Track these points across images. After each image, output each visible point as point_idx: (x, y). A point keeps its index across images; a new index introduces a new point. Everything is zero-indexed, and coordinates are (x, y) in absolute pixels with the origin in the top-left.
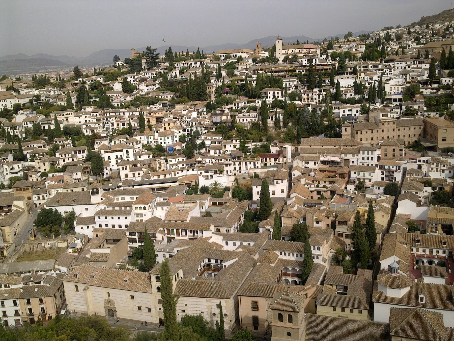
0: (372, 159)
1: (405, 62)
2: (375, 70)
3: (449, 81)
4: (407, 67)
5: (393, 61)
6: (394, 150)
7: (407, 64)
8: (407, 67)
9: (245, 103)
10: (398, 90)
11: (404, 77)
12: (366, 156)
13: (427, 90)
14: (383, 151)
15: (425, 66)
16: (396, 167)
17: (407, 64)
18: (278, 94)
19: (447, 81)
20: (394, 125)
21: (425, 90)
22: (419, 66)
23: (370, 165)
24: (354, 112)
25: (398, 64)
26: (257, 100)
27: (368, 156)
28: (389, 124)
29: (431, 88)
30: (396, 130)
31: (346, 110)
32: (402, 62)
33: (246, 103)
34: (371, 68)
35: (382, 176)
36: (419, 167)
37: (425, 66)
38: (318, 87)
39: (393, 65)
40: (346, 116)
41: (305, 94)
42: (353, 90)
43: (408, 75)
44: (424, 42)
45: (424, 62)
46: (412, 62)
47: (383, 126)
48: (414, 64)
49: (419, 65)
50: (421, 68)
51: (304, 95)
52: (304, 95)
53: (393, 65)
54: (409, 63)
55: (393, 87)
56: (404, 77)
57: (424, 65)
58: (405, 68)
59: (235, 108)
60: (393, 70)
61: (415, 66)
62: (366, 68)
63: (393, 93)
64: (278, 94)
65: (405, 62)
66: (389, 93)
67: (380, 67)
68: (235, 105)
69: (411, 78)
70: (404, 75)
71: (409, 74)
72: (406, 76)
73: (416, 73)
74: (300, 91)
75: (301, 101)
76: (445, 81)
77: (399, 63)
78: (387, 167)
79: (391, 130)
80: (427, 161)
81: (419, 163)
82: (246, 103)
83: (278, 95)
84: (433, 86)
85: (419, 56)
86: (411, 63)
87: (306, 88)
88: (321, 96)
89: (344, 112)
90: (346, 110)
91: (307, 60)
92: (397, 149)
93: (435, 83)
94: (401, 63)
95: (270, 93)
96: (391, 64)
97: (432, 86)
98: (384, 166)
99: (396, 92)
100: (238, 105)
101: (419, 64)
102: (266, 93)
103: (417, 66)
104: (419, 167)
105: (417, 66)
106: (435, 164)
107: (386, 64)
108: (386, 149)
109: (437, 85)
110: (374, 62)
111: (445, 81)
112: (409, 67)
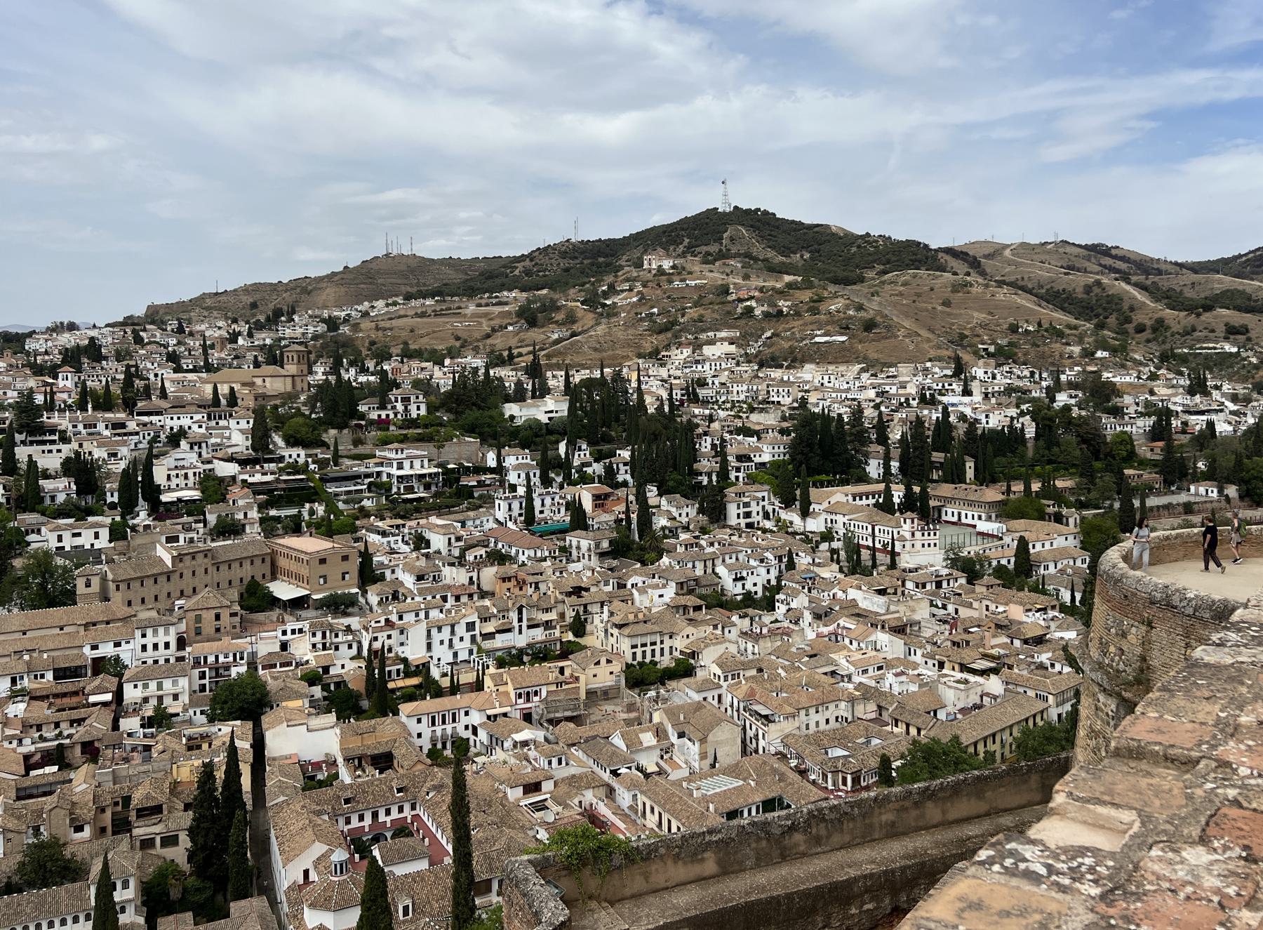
0: (167, 645)
2: (119, 435)
3: (298, 456)
4: (195, 427)
5: (158, 413)
6: (218, 617)
7: (195, 419)
8: (195, 427)
11: (196, 448)
12: (150, 640)
14: (192, 623)
15: (238, 423)
16: (235, 655)
17: (195, 419)
19: (294, 456)
20: (206, 560)
22: (223, 423)
23: (162, 662)
24: (86, 540)
25: (172, 419)
27: (155, 640)
28: (194, 558)
30: (212, 570)
31: (67, 535)
32: (181, 416)
34: (107, 427)
35: (203, 682)
36: (284, 646)
37: (238, 423)
40: (68, 548)
42: (72, 484)
43: (204, 445)
45: (231, 416)
47: (181, 565)
48: (209, 418)
50: (228, 428)
54: (197, 417)
55: (173, 473)
56: (196, 448)
57: (235, 421)
58: (190, 428)
61: (213, 423)
65: (189, 416)
67: (132, 426)
69: (210, 451)
73: (218, 440)
76: (290, 456)
77: (175, 417)
78: (211, 659)
79: (200, 571)
80: (301, 631)
81: (284, 638)
89: (60, 539)
90: (67, 535)
92: (225, 614)
94: (179, 418)
96: (154, 419)
97: (262, 467)
98: (205, 658)
101: (220, 418)
104: (284, 646)
105: (217, 423)
106: (319, 635)
107: (145, 419)
108: (198, 619)
109: (273, 466)
110: (109, 415)
111: (290, 456)
112: (200, 427)
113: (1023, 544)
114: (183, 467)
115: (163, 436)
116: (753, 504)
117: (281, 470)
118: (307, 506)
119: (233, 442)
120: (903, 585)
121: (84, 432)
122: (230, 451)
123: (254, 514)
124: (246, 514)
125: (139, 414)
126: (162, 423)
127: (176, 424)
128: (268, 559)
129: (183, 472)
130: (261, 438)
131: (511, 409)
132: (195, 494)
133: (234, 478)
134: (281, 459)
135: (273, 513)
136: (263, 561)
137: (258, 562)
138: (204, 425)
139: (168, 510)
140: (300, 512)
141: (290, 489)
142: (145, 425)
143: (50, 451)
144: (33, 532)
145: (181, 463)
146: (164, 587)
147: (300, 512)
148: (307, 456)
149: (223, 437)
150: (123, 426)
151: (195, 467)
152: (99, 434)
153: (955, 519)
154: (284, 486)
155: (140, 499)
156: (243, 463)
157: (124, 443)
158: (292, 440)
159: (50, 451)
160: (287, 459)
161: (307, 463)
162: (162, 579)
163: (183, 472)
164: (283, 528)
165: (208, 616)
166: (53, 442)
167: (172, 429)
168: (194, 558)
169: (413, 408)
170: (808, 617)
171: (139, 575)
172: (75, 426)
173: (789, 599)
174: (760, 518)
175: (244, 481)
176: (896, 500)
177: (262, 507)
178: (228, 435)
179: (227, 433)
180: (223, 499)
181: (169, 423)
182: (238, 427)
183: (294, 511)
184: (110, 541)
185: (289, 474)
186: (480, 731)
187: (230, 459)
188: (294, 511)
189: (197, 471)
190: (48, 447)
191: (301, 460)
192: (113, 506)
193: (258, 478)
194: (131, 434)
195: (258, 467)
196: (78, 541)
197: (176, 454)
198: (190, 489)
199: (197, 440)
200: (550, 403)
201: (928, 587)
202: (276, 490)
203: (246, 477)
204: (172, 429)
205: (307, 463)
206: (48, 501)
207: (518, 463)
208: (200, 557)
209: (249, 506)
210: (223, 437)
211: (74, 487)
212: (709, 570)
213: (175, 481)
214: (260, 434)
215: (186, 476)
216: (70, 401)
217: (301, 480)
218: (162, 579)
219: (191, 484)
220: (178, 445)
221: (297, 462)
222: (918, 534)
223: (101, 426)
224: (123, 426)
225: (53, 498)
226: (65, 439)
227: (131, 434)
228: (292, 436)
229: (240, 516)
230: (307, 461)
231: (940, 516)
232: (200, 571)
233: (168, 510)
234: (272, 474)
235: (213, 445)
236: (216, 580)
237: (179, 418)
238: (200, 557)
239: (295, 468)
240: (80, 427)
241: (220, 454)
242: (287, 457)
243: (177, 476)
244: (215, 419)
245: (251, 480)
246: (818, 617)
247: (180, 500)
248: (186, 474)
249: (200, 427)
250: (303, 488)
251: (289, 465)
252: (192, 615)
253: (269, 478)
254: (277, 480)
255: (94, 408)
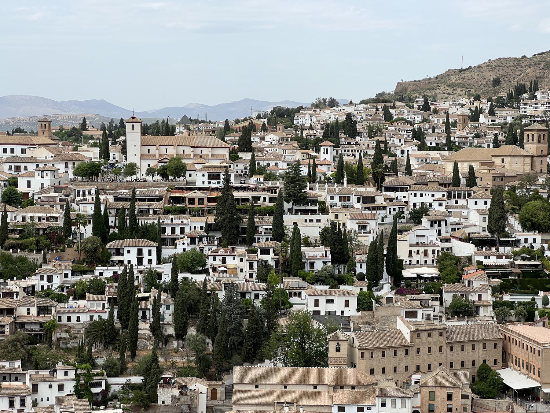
1: (431, 193)
2: (369, 208)
3: (534, 240)
4: (435, 205)
5: (403, 189)
6: (450, 397)
7: (436, 197)
8: (435, 205)
9: (66, 276)
11: (436, 225)
13: (489, 258)
14: (426, 399)
15: (476, 203)
17: (436, 197)
18: (150, 254)
19: (530, 241)
20: (441, 339)
21: (485, 258)
22: (461, 202)
24: (337, 307)
25: (415, 195)
26: (98, 269)
28: (430, 335)
29: (498, 254)
31: (322, 301)
32: (424, 193)
33: (70, 275)
34: (359, 202)
37: (476, 203)
38: (243, 242)
39: (404, 197)
41: (217, 258)
42: (328, 253)
43: (443, 223)
44: (434, 144)
45: (469, 195)
46: (446, 193)
47: (418, 340)
48: (449, 197)
49: (459, 201)
50: (466, 208)
51: (215, 259)
52: (215, 259)
53: (404, 197)
54: (438, 195)
55: (414, 249)
56: (436, 225)
58: (431, 205)
59: (42, 287)
60: (405, 208)
61: (452, 202)
62: (347, 203)
63: (414, 262)
64: (150, 254)
65: (431, 193)
66: (406, 261)
67: (380, 201)
68: (42, 278)
69: (448, 229)
70: (436, 223)
71: (446, 221)
72: (439, 226)
73: (457, 220)
74: (202, 249)
75: (206, 272)
76: (526, 240)
77: (418, 194)
79: (435, 349)
82: (70, 275)
83: (150, 257)
84: (501, 248)
85: (456, 181)
86: (444, 195)
87: (216, 243)
89: (317, 303)
90: (322, 301)
91: (206, 175)
93: (506, 243)
94: (421, 195)
95: (129, 252)
96: (400, 194)
97: (498, 250)
100: (50, 279)
101: (459, 197)
102: (119, 252)
103: (456, 202)
105: (456, 202)
107: (392, 194)
108: (432, 396)
109: (508, 249)
110: (361, 189)
111: (526, 240)
112: (440, 205)
114: (423, 244)
115: (406, 212)
117: (516, 254)
118: (541, 294)
119: (471, 222)
121: (339, 204)
122: (468, 231)
123: (488, 297)
124: (480, 296)
125: (388, 189)
126: (406, 200)
127: (418, 200)
128: (500, 345)
129: (423, 249)
130: (498, 220)
132: (433, 272)
133: (470, 259)
134: (517, 243)
135: (507, 297)
136: (495, 346)
137: (490, 346)
138: (444, 204)
139: (408, 286)
140: (533, 299)
141: (525, 275)
142: (391, 200)
143: (311, 221)
144: (295, 294)
145: (421, 240)
146: (402, 360)
147: (533, 299)
148: (544, 241)
149: (461, 217)
150: (372, 200)
151: (434, 245)
152: (352, 207)
154: (518, 271)
155: (385, 272)
156: (480, 244)
157: (373, 217)
158: (528, 224)
159: (311, 221)
160: (523, 244)
161: (542, 250)
162: (401, 352)
163: (423, 249)
164: (516, 315)
165: (442, 395)
166: (313, 212)
167: (415, 205)
168: (430, 335)
171: (381, 345)
172: (332, 198)
175: (480, 263)
177: (496, 291)
178: (466, 214)
179: (465, 213)
180: (459, 280)
181: (412, 200)
182: (476, 207)
183: (526, 299)
184: (358, 310)
185: (524, 259)
187: (468, 240)
188: (526, 299)
189: (436, 249)
190: (309, 217)
191: (537, 246)
192: (361, 277)
193: (493, 261)
194: (379, 208)
195: (493, 249)
196: (331, 307)
197: (418, 230)
198: (428, 266)
199: (437, 218)
202: (511, 274)
203: (481, 258)
204: (415, 205)
205: (542, 250)
206: (308, 268)
208: (436, 334)
209: (483, 288)
210: (461, 217)
211: (329, 256)
213: (415, 257)
214: (497, 215)
215: (426, 254)
216: (329, 174)
217: (536, 266)
218: (401, 352)
219: (430, 262)
220: (419, 222)
221: (532, 247)
223: (354, 199)
224: (372, 200)
225: (312, 264)
226: (324, 210)
227: (379, 208)
228: (529, 220)
229: (474, 298)
230: (543, 247)
232: (435, 349)
233: (408, 286)
234: (507, 257)
235: (451, 224)
236: (449, 360)
237: (421, 195)
238: (436, 334)
239: (530, 253)
240: (337, 199)
241: (457, 234)
242: (523, 241)
243: (418, 252)
244: (454, 197)
245: (486, 262)
247: (419, 277)
248: (426, 251)
249: (440, 205)
250: (538, 275)
251: (524, 250)
252: (426, 391)
253: (504, 261)
254: (512, 265)
255: (349, 182)
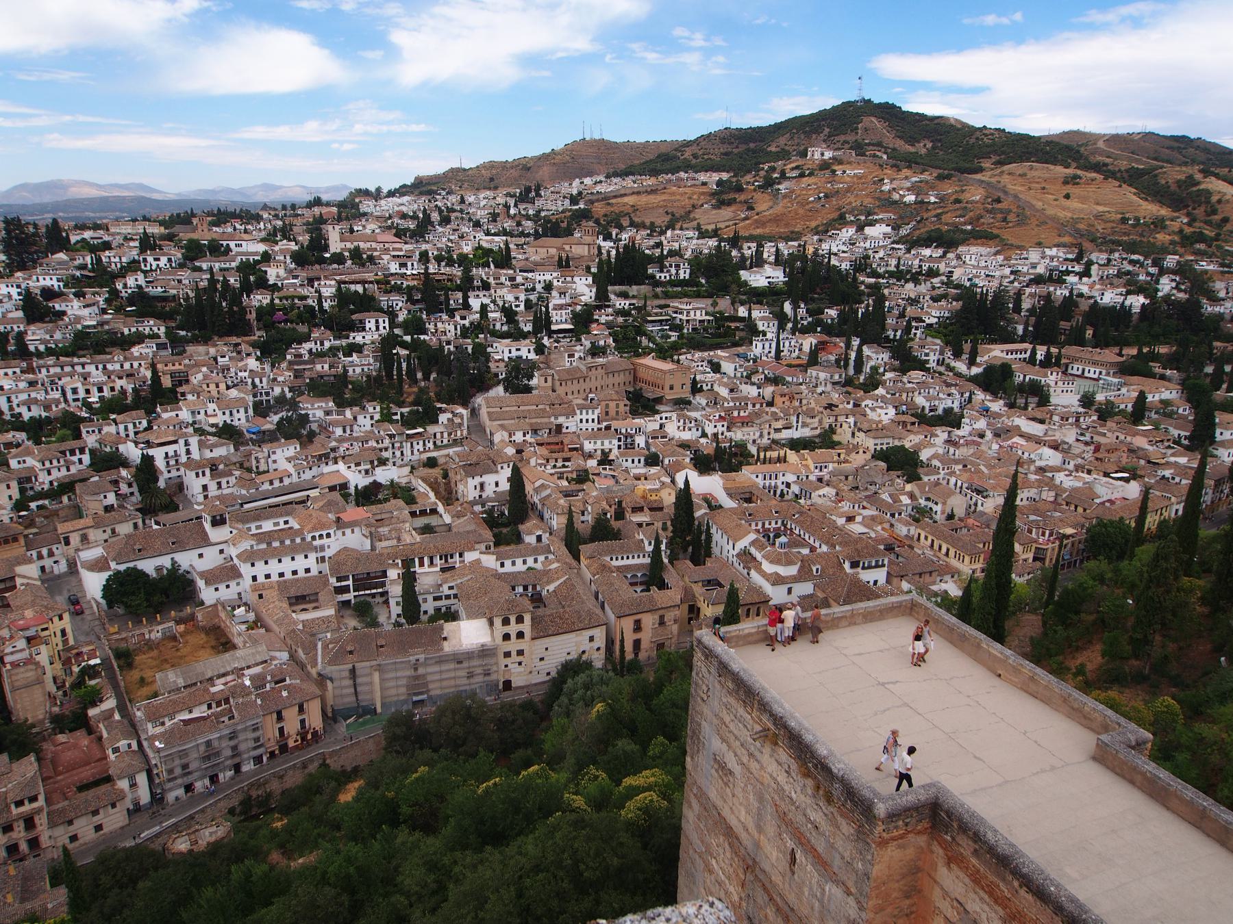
10: (561, 316)
88: (458, 327)
99: (559, 320)
113: (1142, 396)
116: (932, 354)
120: (1051, 418)
131: (744, 275)
153: (1079, 373)
169: (681, 272)
170: (989, 435)
173: (973, 422)
174: (935, 365)
176: (1039, 357)
186: (792, 486)
200: (768, 270)
201: (1070, 420)
207: (759, 314)
212: (909, 399)
222: (1060, 383)
231: (1067, 370)
246: (997, 435)
